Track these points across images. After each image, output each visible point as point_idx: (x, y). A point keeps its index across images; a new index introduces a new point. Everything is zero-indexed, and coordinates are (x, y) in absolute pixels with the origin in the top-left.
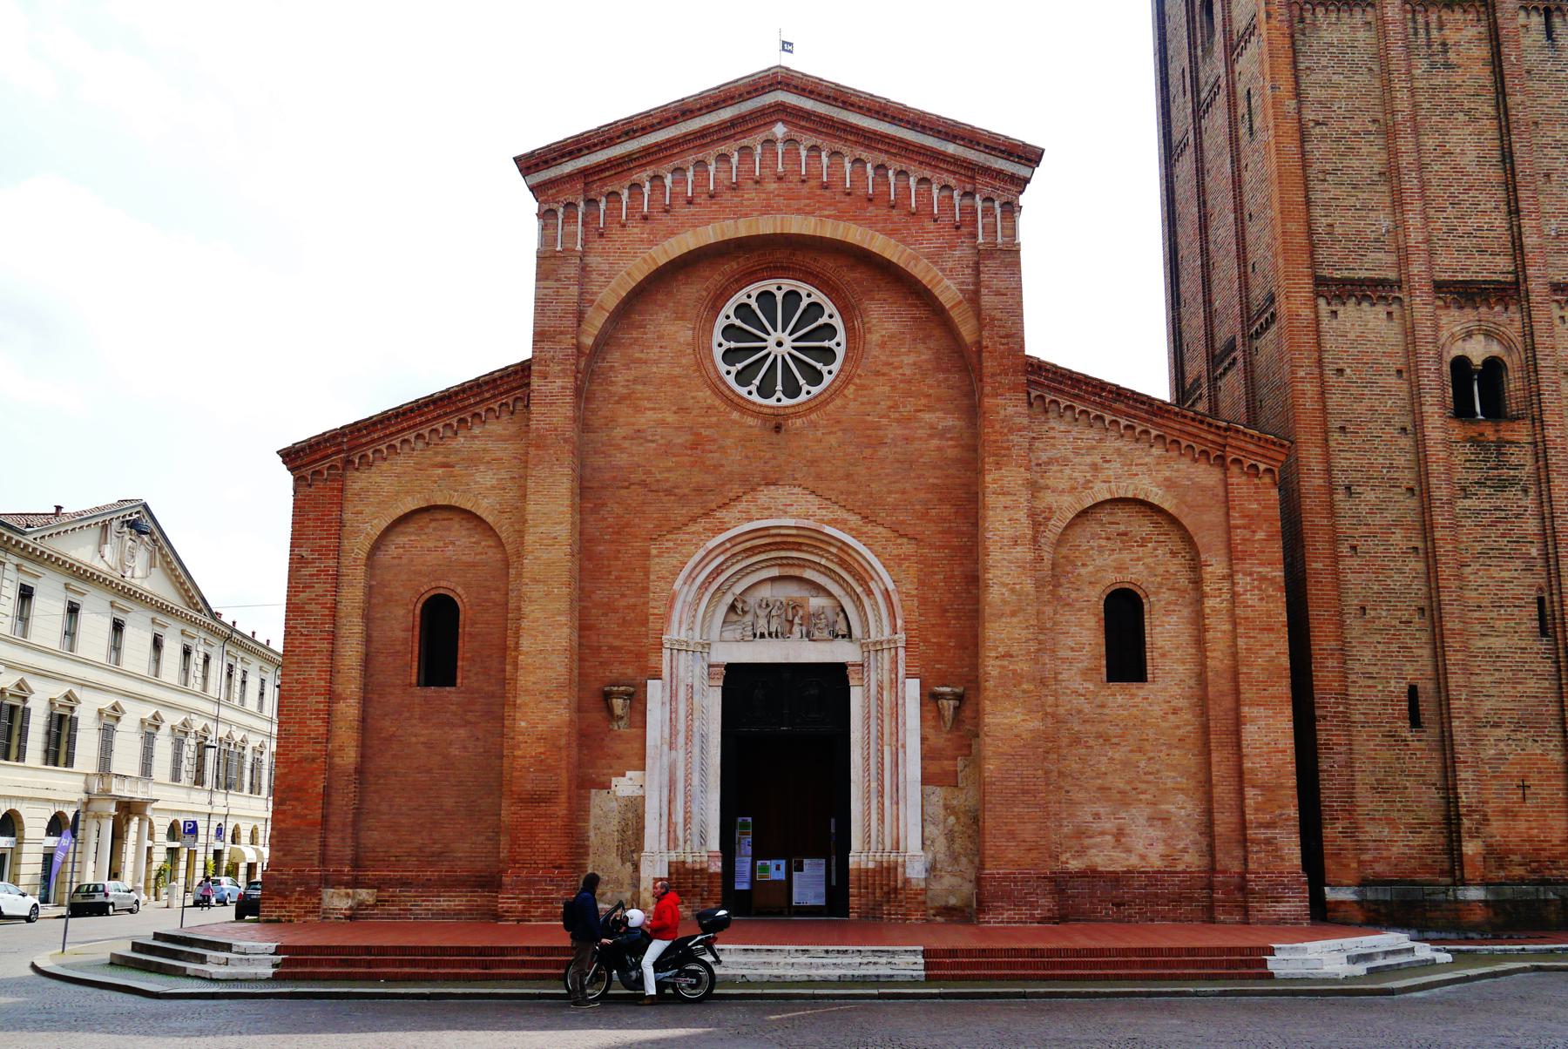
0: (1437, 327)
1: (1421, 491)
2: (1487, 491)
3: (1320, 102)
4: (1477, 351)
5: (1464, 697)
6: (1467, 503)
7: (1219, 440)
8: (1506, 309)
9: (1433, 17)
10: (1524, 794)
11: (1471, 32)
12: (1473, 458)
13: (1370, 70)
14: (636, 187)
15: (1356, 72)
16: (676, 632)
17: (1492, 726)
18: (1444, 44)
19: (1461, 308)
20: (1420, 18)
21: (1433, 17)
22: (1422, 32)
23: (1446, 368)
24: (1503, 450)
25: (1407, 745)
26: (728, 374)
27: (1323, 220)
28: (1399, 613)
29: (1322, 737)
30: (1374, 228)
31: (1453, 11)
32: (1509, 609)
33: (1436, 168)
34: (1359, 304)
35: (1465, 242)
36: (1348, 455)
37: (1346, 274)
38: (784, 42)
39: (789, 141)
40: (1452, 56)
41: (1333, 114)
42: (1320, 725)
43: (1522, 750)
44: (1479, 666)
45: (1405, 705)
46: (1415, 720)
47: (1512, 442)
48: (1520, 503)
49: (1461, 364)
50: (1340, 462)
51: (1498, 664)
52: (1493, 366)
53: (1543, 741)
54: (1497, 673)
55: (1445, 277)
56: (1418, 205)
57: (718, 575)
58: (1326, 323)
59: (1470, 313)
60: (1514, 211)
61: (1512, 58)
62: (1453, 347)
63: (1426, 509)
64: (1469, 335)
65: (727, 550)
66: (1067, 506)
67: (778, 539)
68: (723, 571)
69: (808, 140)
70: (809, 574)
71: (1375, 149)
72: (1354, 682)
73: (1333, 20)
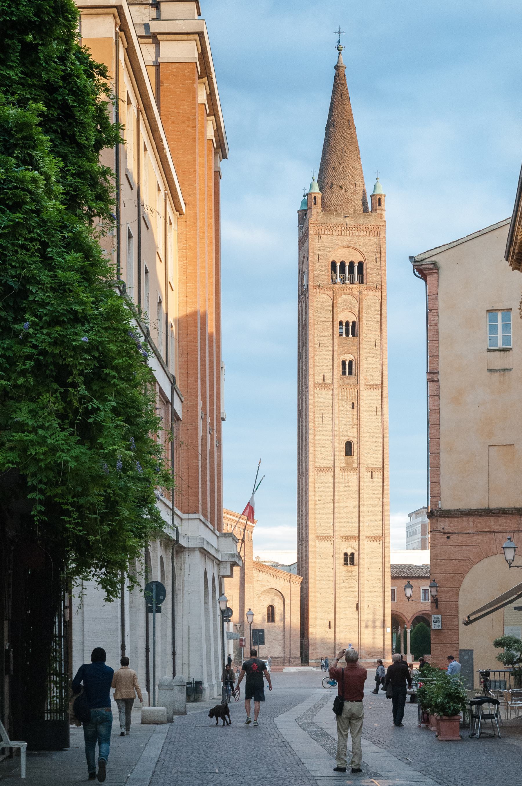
1: (334, 582)
9: (346, 474)
21: (346, 474)
37: (322, 535)
42: (310, 629)
46: (330, 628)
49: (346, 554)
52: (352, 554)
60: (359, 520)
63: (335, 585)
64: (348, 547)
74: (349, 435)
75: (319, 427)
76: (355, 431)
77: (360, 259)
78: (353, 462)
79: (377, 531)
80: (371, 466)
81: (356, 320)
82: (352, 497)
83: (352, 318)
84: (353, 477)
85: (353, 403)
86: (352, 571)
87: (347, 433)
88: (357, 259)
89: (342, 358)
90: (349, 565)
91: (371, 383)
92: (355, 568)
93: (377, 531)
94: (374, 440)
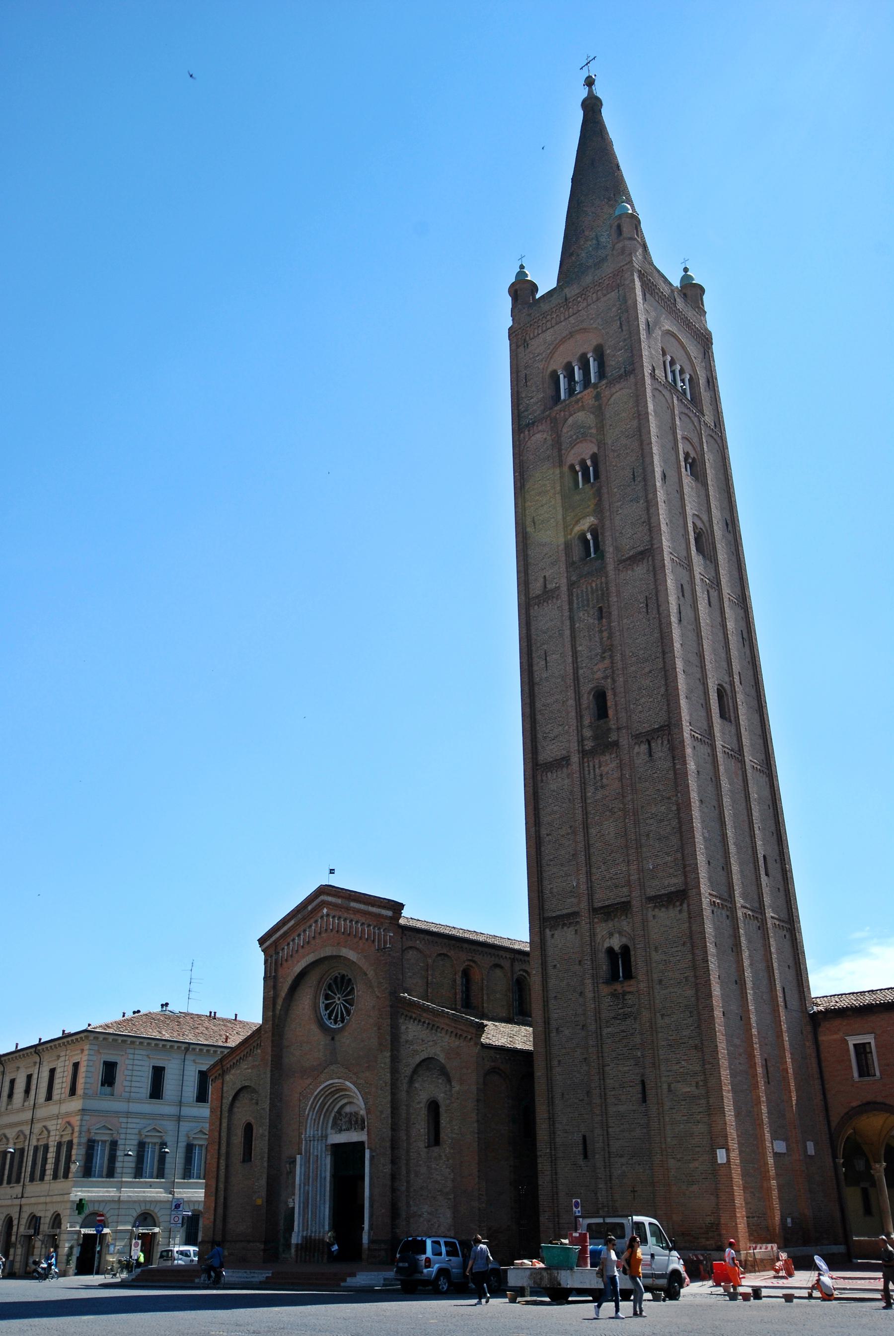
0: (593, 935)
2: (618, 1022)
3: (548, 824)
4: (616, 943)
5: (601, 1141)
6: (609, 1029)
7: (455, 1025)
8: (627, 917)
9: (597, 761)
10: (634, 1196)
11: (613, 765)
12: (612, 1004)
13: (570, 799)
14: (289, 944)
15: (563, 803)
16: (310, 1132)
17: (620, 1157)
18: (601, 775)
19: (606, 921)
20: (591, 764)
22: (592, 771)
23: (602, 957)
24: (626, 997)
25: (581, 1169)
26: (324, 1013)
27: (549, 887)
28: (578, 1095)
29: (540, 1166)
30: (569, 885)
31: (605, 755)
32: (627, 1089)
33: (597, 845)
34: (563, 928)
35: (609, 883)
36: (558, 1011)
37: (558, 913)
38: (331, 870)
39: (328, 915)
40: (605, 780)
41: (553, 828)
42: (539, 1160)
43: (634, 1170)
44: (614, 1122)
45: (581, 1147)
46: (586, 1156)
47: (629, 992)
48: (633, 1026)
49: (610, 951)
50: (554, 1015)
51: (623, 1120)
52: (625, 949)
53: (643, 1164)
54: (622, 1126)
55: (600, 905)
56: (584, 870)
57: (325, 1106)
58: (550, 942)
59: (610, 924)
61: (627, 776)
62: (605, 943)
64: (611, 935)
65: (323, 1094)
66: (410, 1061)
67: (338, 1088)
68: (326, 1104)
69: (332, 913)
70: (355, 1101)
71: (571, 842)
72: (559, 1135)
73: (555, 777)
74: (596, 676)
75: (541, 679)
76: (607, 662)
77: (594, 340)
78: (609, 730)
79: (674, 880)
80: (646, 727)
81: (596, 450)
82: (610, 811)
83: (586, 450)
84: (608, 764)
85: (600, 609)
86: (624, 994)
87: (593, 673)
88: (586, 344)
89: (577, 529)
90: (621, 979)
91: (631, 554)
92: (630, 986)
93: (674, 880)
94: (647, 670)
